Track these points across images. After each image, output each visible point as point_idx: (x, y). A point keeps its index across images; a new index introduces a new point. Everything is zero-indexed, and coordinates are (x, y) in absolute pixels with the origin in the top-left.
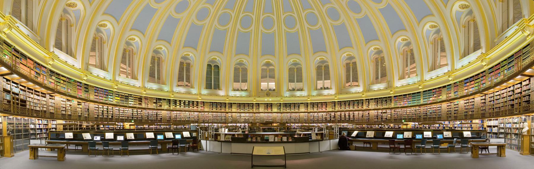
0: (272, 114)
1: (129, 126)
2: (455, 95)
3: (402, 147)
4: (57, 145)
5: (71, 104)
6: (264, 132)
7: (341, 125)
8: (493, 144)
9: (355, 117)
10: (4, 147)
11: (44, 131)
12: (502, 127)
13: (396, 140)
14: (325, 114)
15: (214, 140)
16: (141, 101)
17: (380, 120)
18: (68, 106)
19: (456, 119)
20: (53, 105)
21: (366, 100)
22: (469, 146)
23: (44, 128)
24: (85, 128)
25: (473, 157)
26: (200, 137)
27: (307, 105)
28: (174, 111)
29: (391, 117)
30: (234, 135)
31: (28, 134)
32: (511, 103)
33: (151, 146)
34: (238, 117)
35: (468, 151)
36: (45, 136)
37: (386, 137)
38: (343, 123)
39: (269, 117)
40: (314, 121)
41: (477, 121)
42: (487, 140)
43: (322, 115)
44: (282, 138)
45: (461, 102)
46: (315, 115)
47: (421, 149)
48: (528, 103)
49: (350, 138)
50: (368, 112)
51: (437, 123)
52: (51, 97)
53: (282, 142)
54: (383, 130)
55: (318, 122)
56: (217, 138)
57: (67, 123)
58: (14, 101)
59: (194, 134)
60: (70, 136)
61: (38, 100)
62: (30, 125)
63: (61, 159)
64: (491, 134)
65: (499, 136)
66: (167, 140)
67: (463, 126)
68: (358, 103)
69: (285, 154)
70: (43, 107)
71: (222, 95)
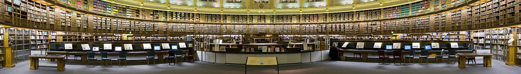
0: (265, 26)
1: (127, 38)
2: (443, 7)
3: (391, 57)
4: (57, 56)
5: (71, 16)
6: (258, 43)
7: (332, 36)
8: (479, 54)
9: (345, 29)
10: (5, 58)
11: (44, 42)
12: (488, 38)
13: (385, 51)
14: (317, 25)
15: (209, 51)
16: (139, 13)
17: (369, 32)
18: (68, 17)
19: (443, 30)
20: (53, 17)
21: (356, 12)
22: (456, 57)
23: (45, 39)
24: (84, 39)
25: (460, 68)
26: (196, 48)
27: (299, 17)
28: (170, 22)
29: (380, 29)
30: (228, 46)
31: (29, 45)
32: (497, 15)
33: (148, 57)
34: (232, 29)
35: (455, 62)
36: (45, 47)
37: (374, 48)
38: (334, 34)
39: (262, 29)
40: (305, 32)
41: (464, 32)
42: (473, 51)
43: (314, 26)
44: (275, 49)
45: (449, 14)
46: (307, 27)
47: (410, 59)
48: (512, 16)
49: (341, 49)
50: (358, 24)
51: (425, 35)
52: (51, 9)
53: (275, 53)
54: (373, 42)
55: (310, 33)
56: (212, 49)
57: (66, 34)
58: (15, 13)
59: (190, 45)
60: (69, 47)
61: (39, 12)
62: (31, 37)
63: (61, 69)
64: (477, 45)
65: (485, 47)
66: (163, 50)
67: (451, 38)
69: (278, 64)
70: (43, 19)
71: (217, 7)
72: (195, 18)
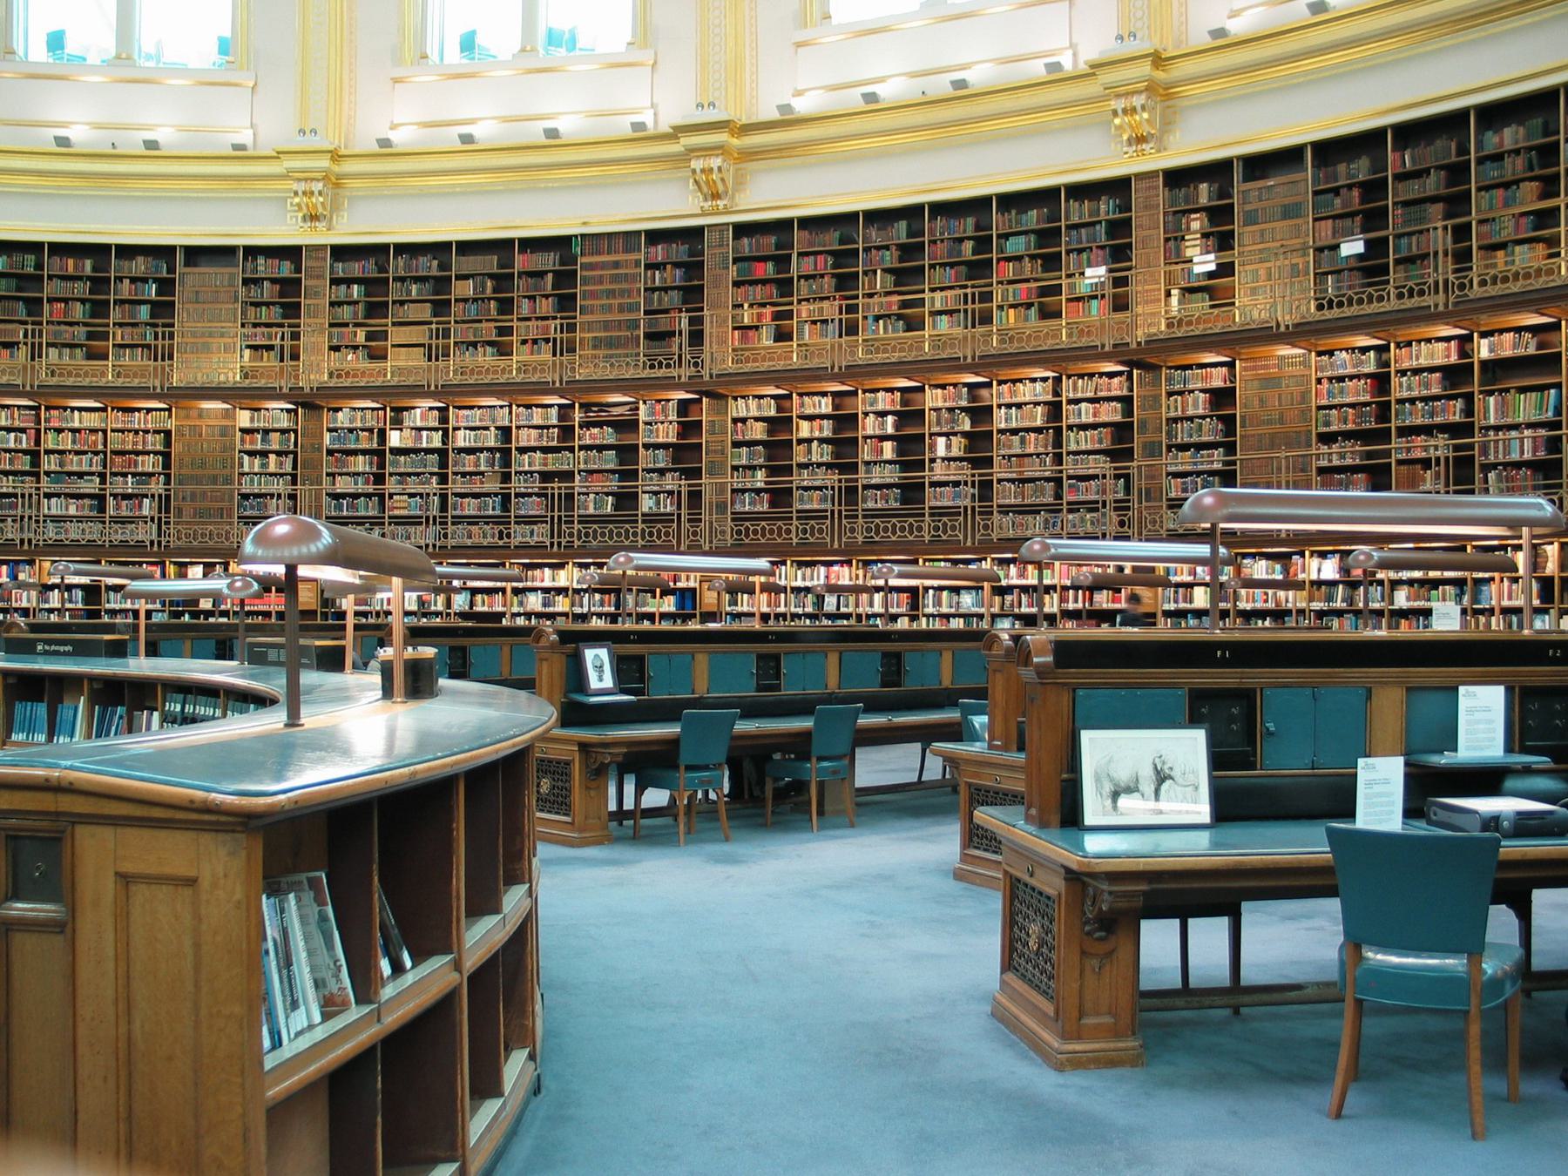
27: (290, 286)
46: (395, 439)
50: (1217, 379)
68: (1048, 236)
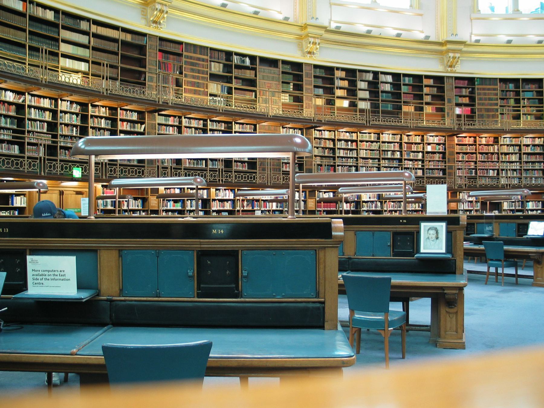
72: (450, 101)
